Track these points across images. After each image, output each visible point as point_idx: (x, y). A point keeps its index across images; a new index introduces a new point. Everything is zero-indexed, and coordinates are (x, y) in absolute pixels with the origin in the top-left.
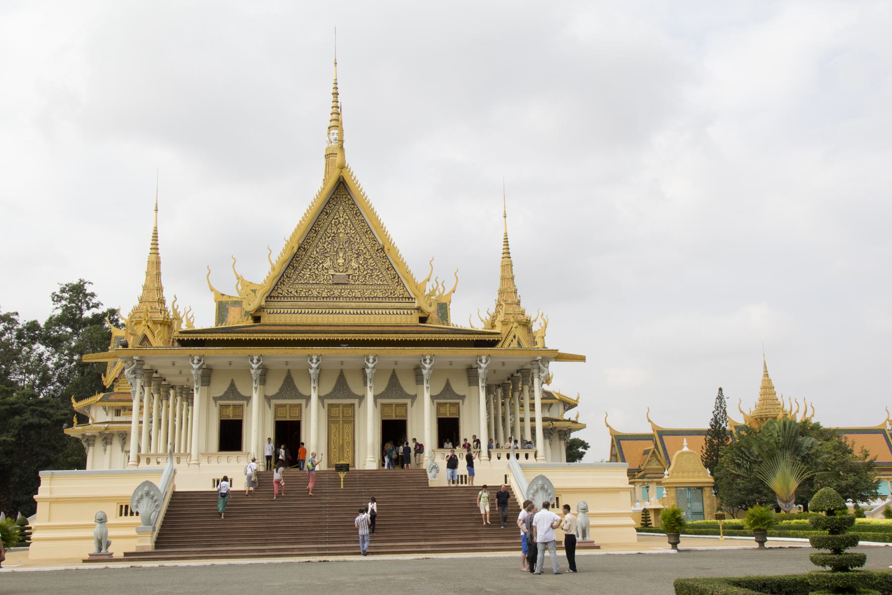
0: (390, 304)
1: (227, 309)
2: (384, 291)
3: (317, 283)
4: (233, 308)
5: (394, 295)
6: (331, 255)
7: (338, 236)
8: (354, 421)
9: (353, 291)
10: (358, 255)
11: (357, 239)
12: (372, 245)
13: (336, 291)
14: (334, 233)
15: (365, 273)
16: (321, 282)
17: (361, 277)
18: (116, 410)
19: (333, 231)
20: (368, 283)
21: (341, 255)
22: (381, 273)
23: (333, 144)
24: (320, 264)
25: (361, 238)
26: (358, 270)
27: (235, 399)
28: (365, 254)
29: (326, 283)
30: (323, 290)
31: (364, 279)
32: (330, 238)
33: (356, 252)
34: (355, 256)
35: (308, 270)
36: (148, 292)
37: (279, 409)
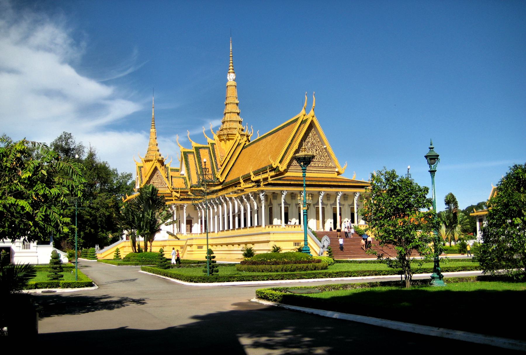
1: (187, 155)
10: (316, 150)
21: (310, 150)
23: (231, 80)
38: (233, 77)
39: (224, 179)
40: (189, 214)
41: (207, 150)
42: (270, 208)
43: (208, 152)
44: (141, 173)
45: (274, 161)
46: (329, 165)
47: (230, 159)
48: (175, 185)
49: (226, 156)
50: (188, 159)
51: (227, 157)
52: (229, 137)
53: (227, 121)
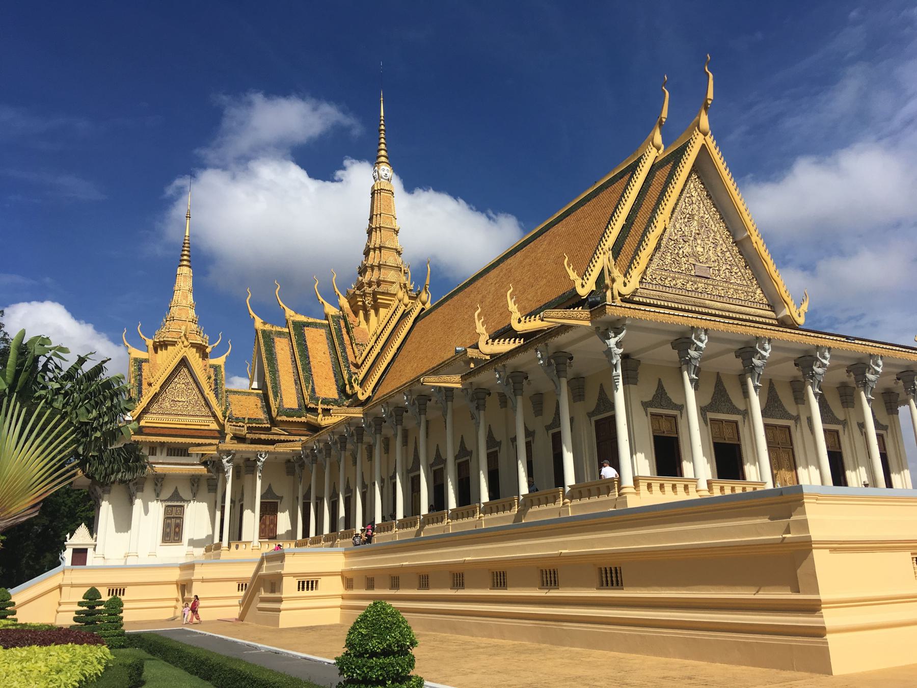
0: (753, 310)
1: (273, 339)
2: (745, 294)
3: (678, 272)
4: (278, 339)
5: (754, 299)
6: (689, 240)
7: (693, 218)
8: (793, 449)
9: (716, 287)
10: (716, 245)
11: (711, 226)
12: (727, 236)
13: (700, 285)
14: (688, 213)
15: (724, 268)
16: (684, 272)
17: (721, 272)
18: (150, 448)
19: (688, 212)
20: (728, 280)
22: (740, 271)
24: (680, 249)
25: (716, 226)
26: (717, 263)
27: (668, 408)
28: (722, 244)
29: (688, 273)
30: (687, 282)
31: (724, 275)
32: (686, 220)
33: (714, 242)
34: (713, 246)
35: (669, 254)
36: (179, 309)
37: (735, 424)
38: (386, 172)
39: (369, 393)
40: (270, 487)
41: (323, 332)
42: (596, 422)
43: (324, 335)
44: (141, 375)
45: (583, 275)
46: (757, 296)
47: (382, 349)
48: (236, 411)
49: (372, 343)
50: (274, 347)
51: (373, 347)
52: (379, 301)
53: (372, 267)
